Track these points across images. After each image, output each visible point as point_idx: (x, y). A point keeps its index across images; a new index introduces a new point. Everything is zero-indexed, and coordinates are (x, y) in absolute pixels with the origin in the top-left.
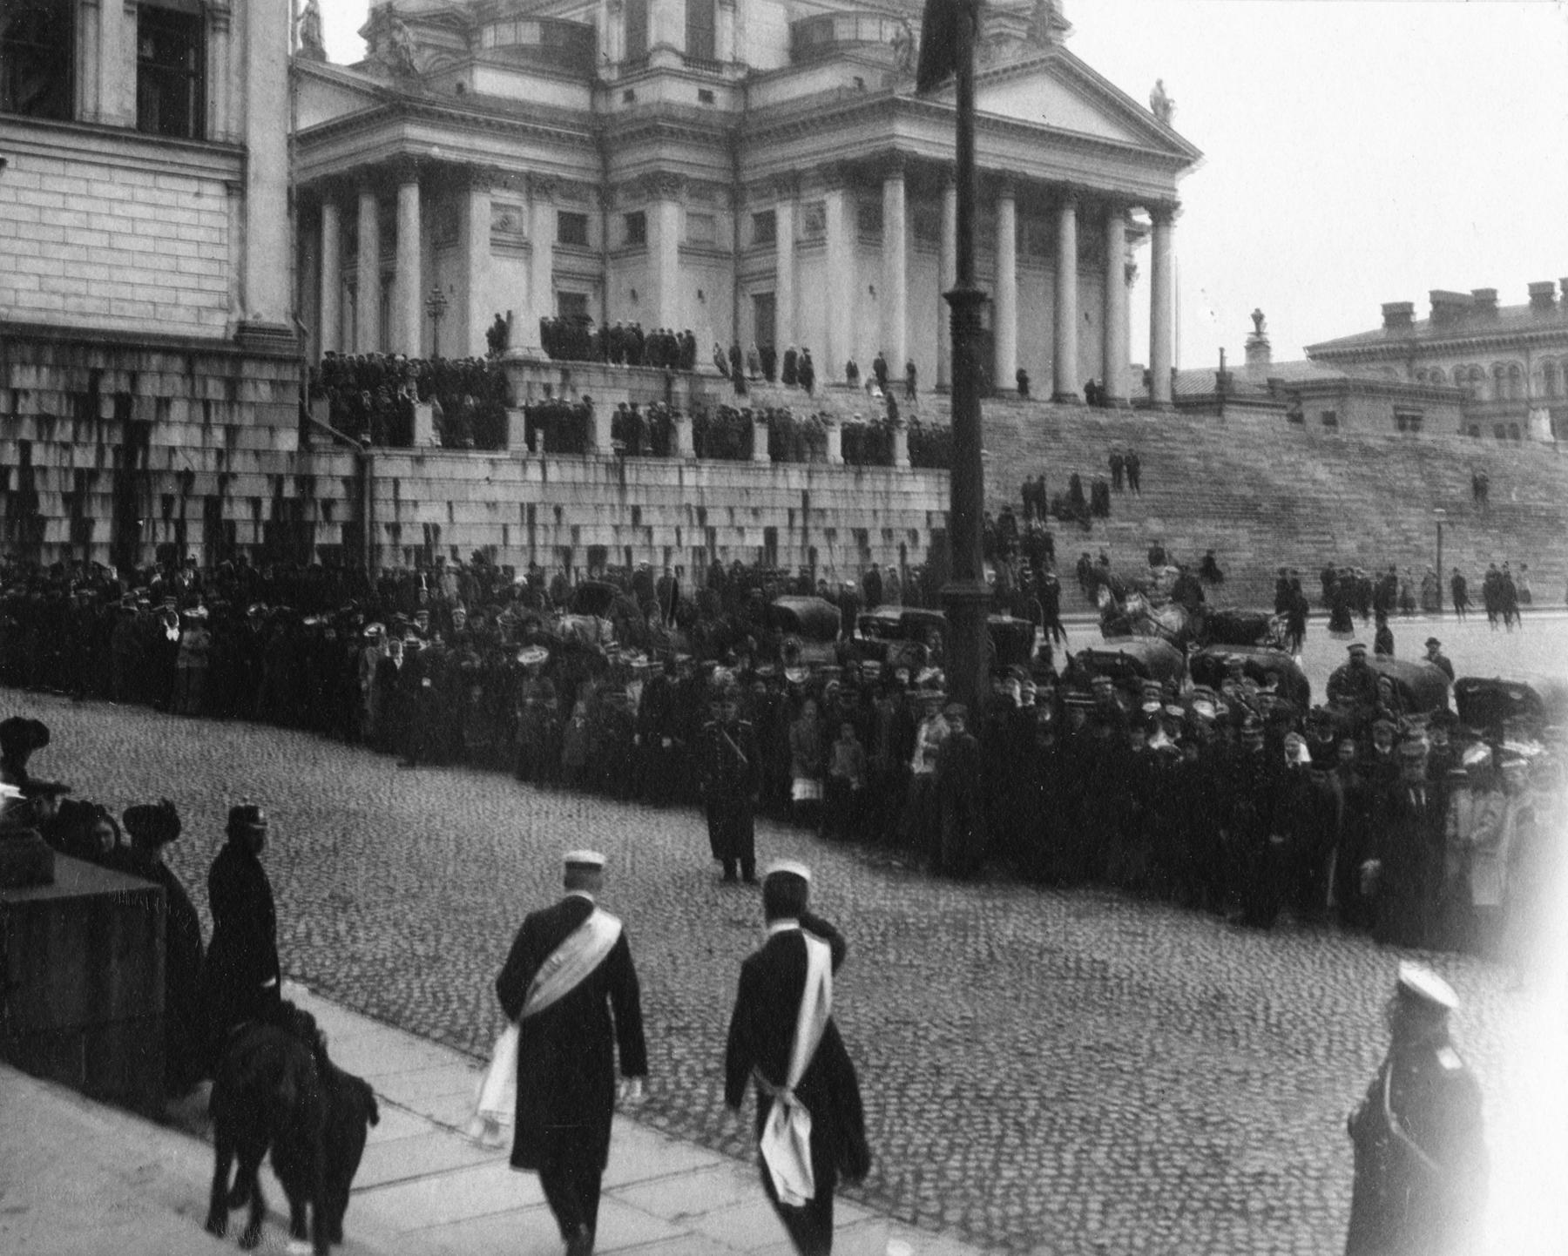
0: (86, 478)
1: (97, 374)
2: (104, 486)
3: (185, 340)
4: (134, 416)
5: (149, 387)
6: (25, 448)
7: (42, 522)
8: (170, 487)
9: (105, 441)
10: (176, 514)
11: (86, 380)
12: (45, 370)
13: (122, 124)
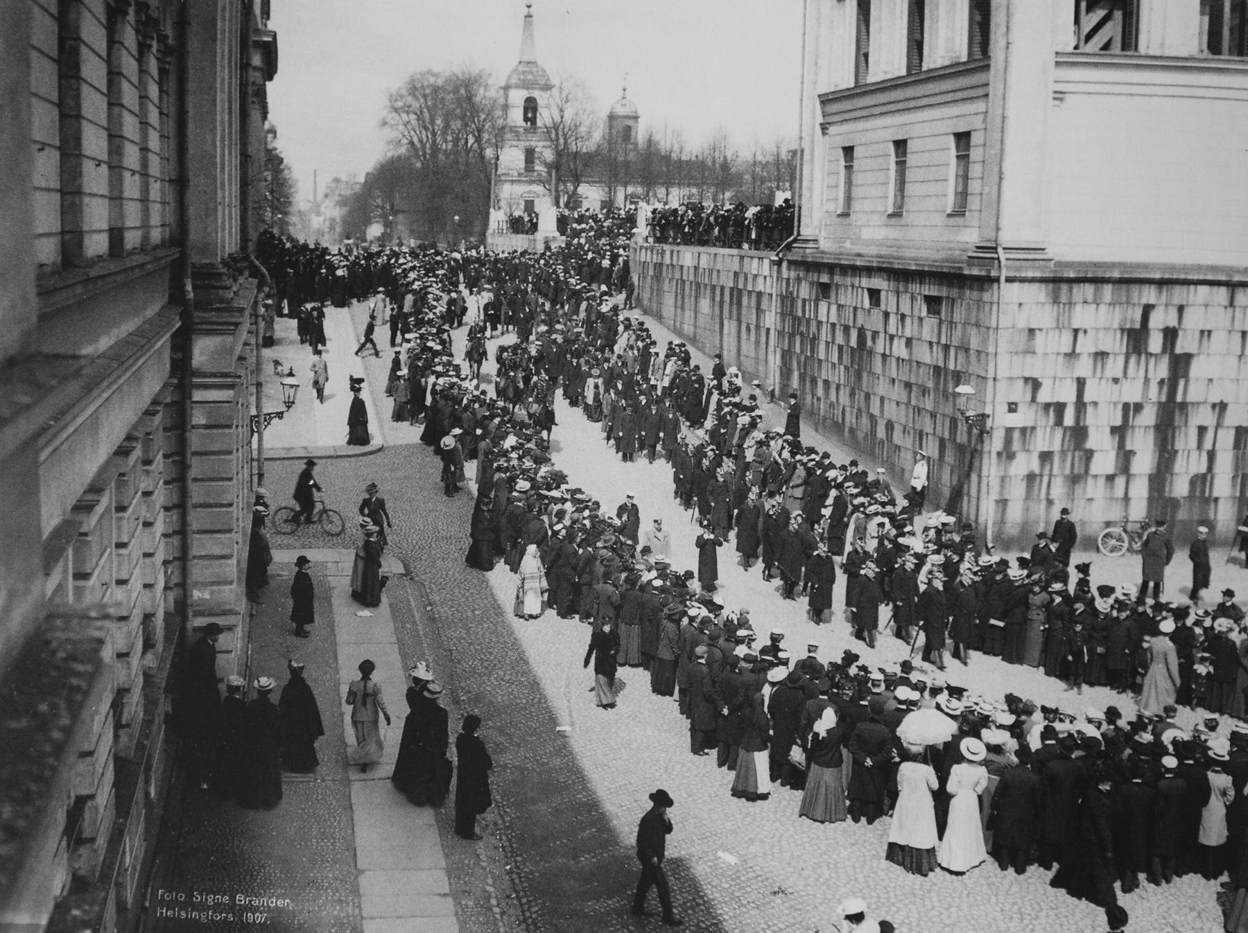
0: (1130, 409)
1: (1148, 309)
2: (1148, 417)
3: (1231, 270)
4: (1179, 350)
5: (1194, 320)
6: (1081, 383)
7: (1089, 454)
8: (1205, 416)
9: (1150, 375)
10: (1208, 445)
11: (1138, 314)
12: (1103, 308)
13: (1184, 54)
